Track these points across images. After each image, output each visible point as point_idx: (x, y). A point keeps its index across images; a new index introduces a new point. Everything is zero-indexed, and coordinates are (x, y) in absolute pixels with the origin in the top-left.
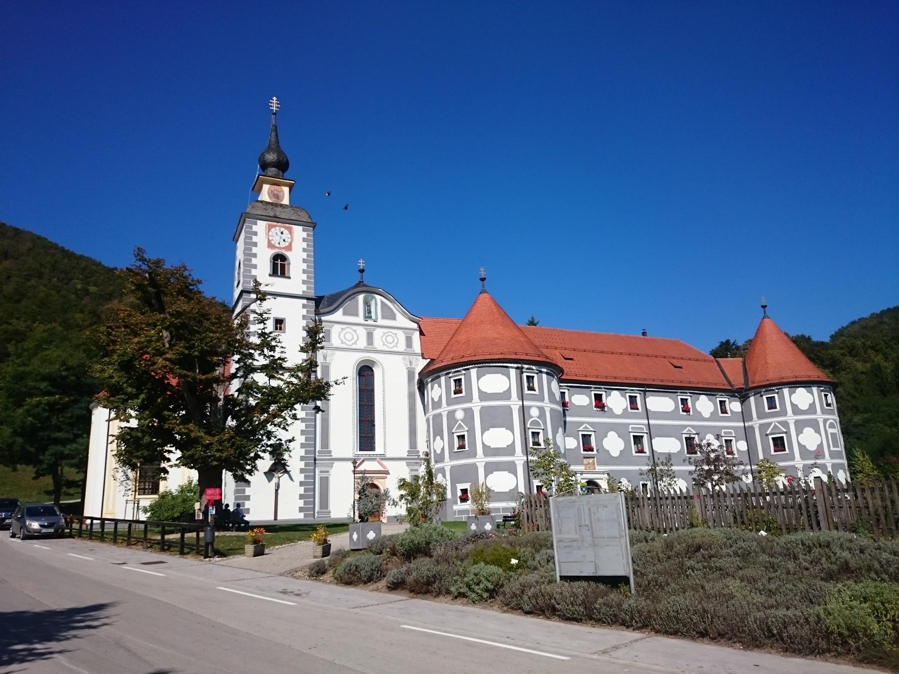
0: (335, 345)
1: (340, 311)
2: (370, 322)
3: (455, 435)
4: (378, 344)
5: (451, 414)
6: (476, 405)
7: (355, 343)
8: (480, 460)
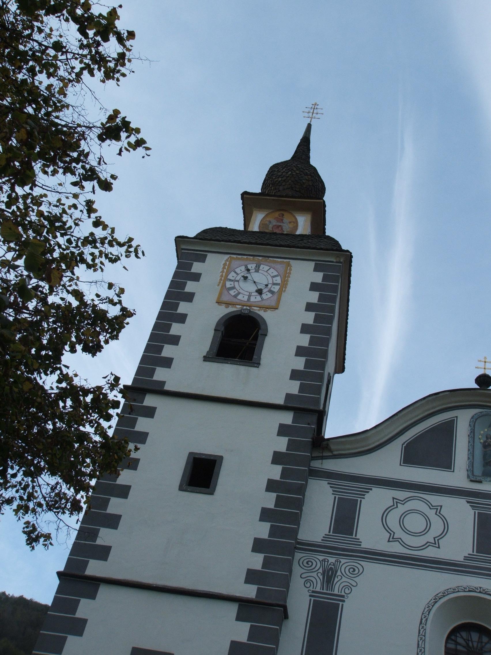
0: (367, 544)
1: (395, 450)
7: (436, 543)
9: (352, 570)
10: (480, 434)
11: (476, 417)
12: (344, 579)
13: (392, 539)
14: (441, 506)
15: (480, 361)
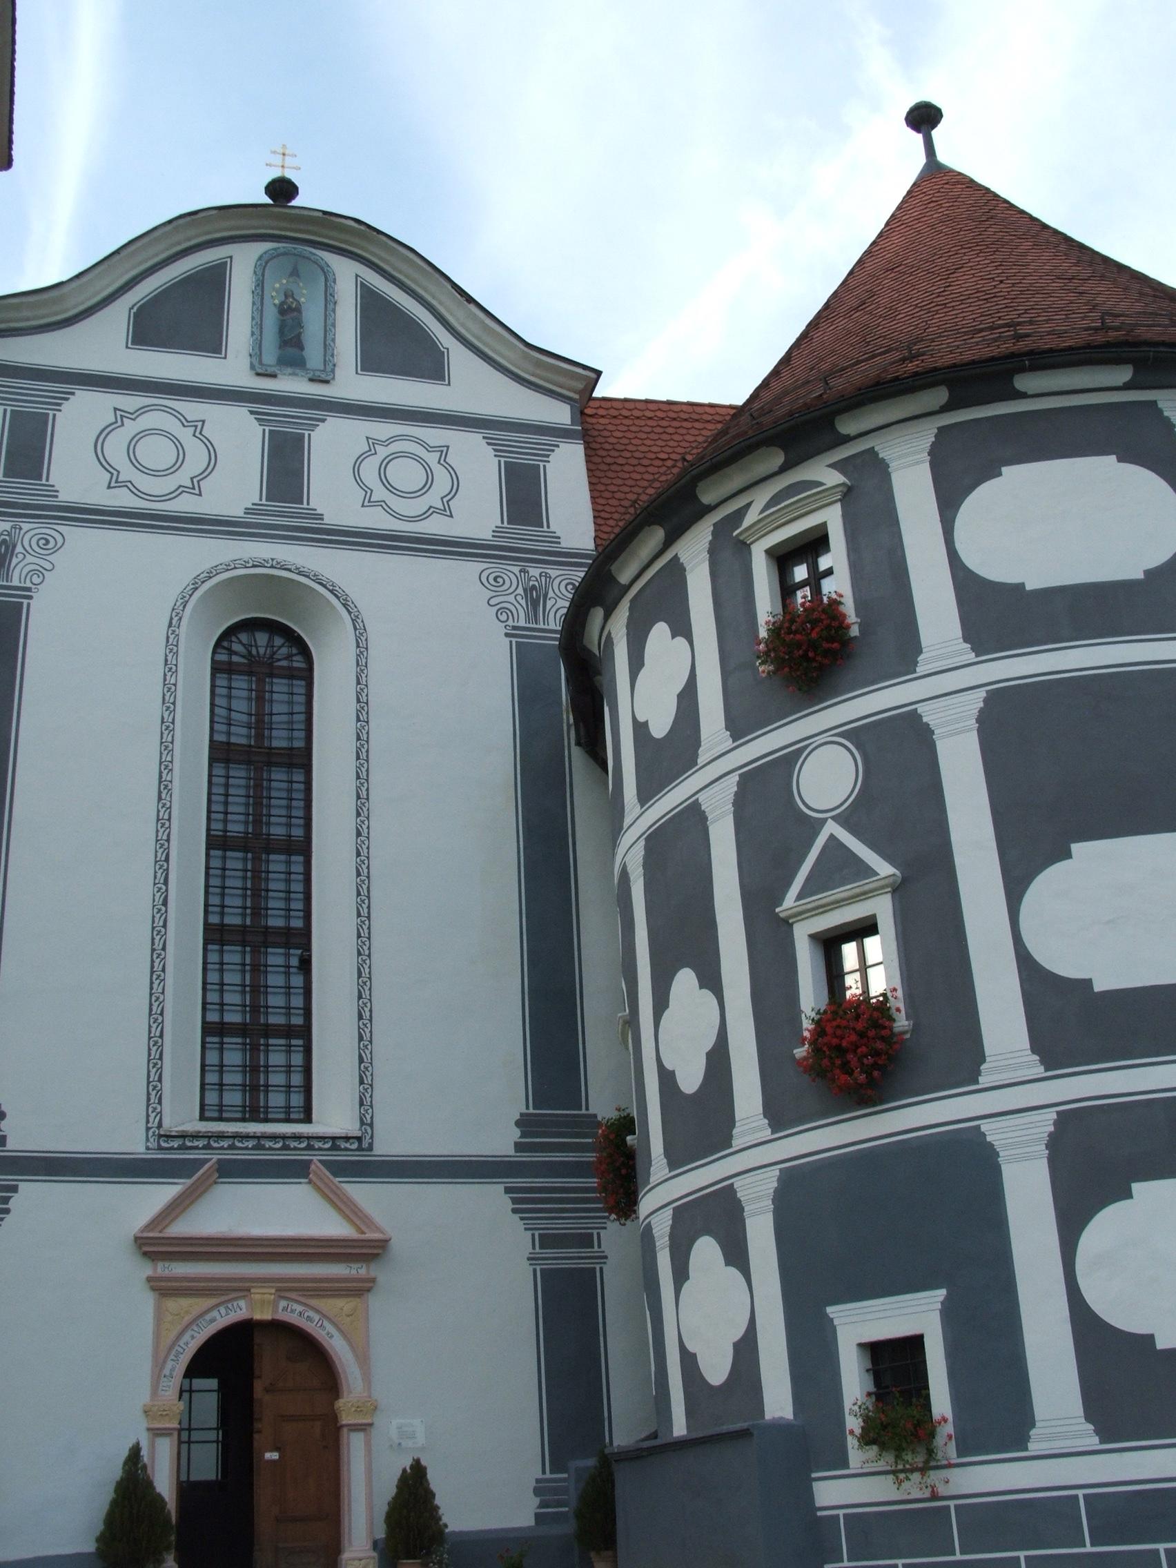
1: (118, 317)
2: (291, 384)
3: (802, 933)
4: (331, 492)
5: (767, 796)
6: (947, 686)
8: (1012, 1102)
9: (43, 542)
10: (274, 289)
11: (266, 257)
12: (29, 559)
13: (115, 482)
14: (203, 422)
15: (274, 152)
